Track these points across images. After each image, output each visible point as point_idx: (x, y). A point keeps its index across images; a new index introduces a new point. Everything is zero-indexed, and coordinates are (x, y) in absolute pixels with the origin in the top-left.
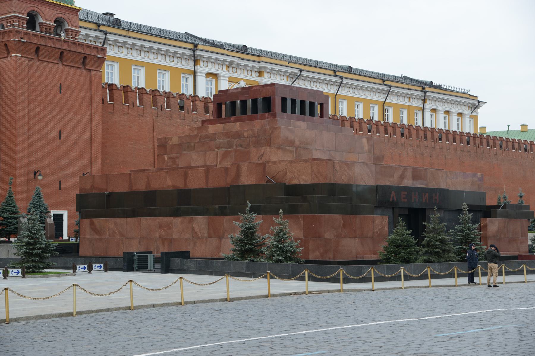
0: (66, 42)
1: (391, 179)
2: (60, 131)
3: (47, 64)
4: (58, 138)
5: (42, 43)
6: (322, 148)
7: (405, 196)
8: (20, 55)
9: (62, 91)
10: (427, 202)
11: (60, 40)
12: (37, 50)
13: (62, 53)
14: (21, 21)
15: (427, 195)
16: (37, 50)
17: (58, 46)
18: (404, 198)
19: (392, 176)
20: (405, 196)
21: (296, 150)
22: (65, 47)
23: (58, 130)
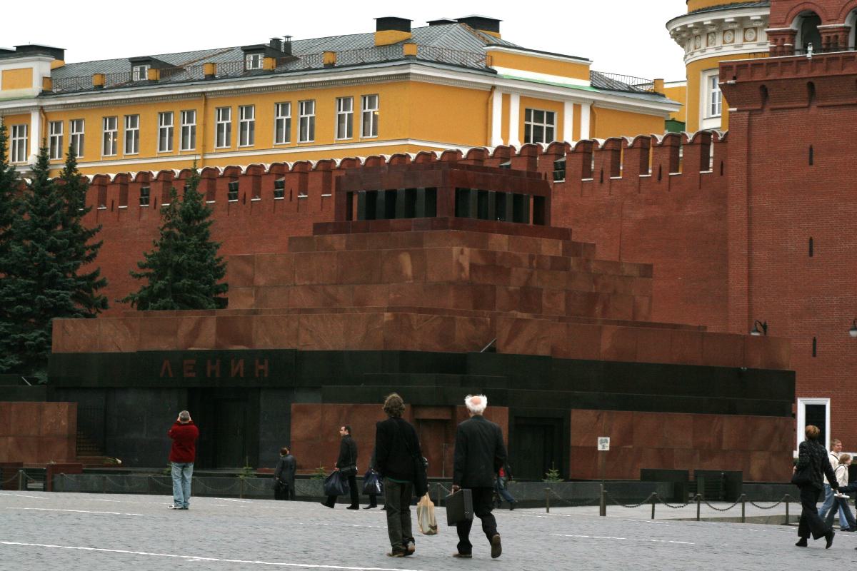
0: (815, 60)
1: (172, 340)
2: (811, 240)
3: (785, 113)
4: (807, 253)
5: (771, 77)
6: (307, 283)
7: (191, 368)
8: (735, 109)
9: (815, 160)
10: (242, 375)
11: (805, 60)
12: (764, 90)
14: (780, 39)
15: (241, 363)
16: (764, 90)
17: (804, 74)
18: (189, 371)
19: (174, 333)
20: (191, 368)
21: (257, 292)
22: (817, 73)
23: (807, 238)
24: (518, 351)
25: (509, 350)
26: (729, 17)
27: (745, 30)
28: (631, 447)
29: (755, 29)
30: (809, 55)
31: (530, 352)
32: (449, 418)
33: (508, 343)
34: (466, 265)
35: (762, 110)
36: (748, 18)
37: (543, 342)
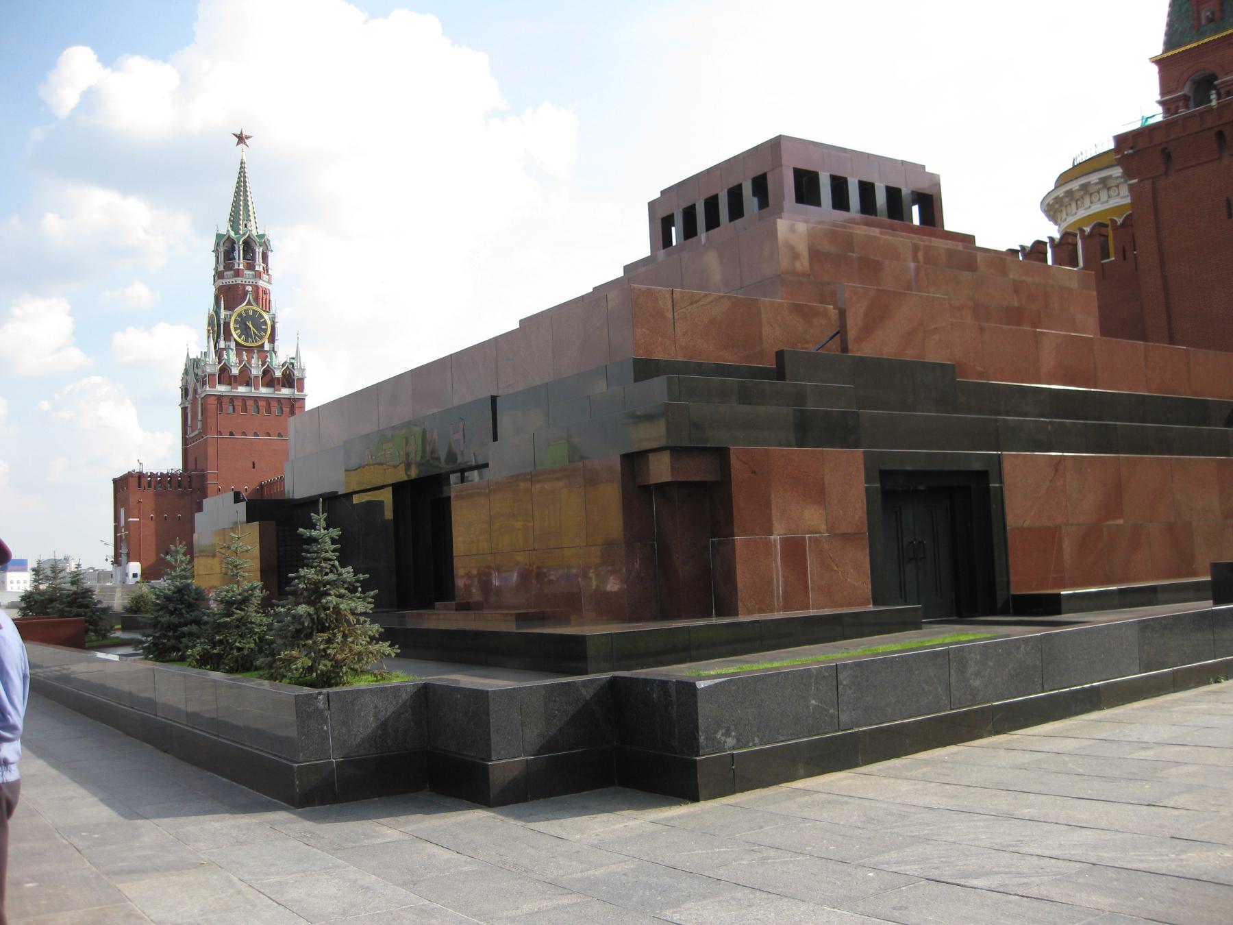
0: (1221, 107)
5: (1172, 137)
11: (1211, 109)
13: (1220, 135)
14: (1173, 107)
24: (887, 352)
25: (866, 350)
26: (1094, 178)
27: (1109, 189)
28: (1121, 521)
29: (1117, 186)
30: (1214, 103)
31: (910, 355)
32: (710, 478)
33: (868, 329)
34: (803, 248)
35: (1166, 174)
36: (1110, 176)
37: (936, 337)
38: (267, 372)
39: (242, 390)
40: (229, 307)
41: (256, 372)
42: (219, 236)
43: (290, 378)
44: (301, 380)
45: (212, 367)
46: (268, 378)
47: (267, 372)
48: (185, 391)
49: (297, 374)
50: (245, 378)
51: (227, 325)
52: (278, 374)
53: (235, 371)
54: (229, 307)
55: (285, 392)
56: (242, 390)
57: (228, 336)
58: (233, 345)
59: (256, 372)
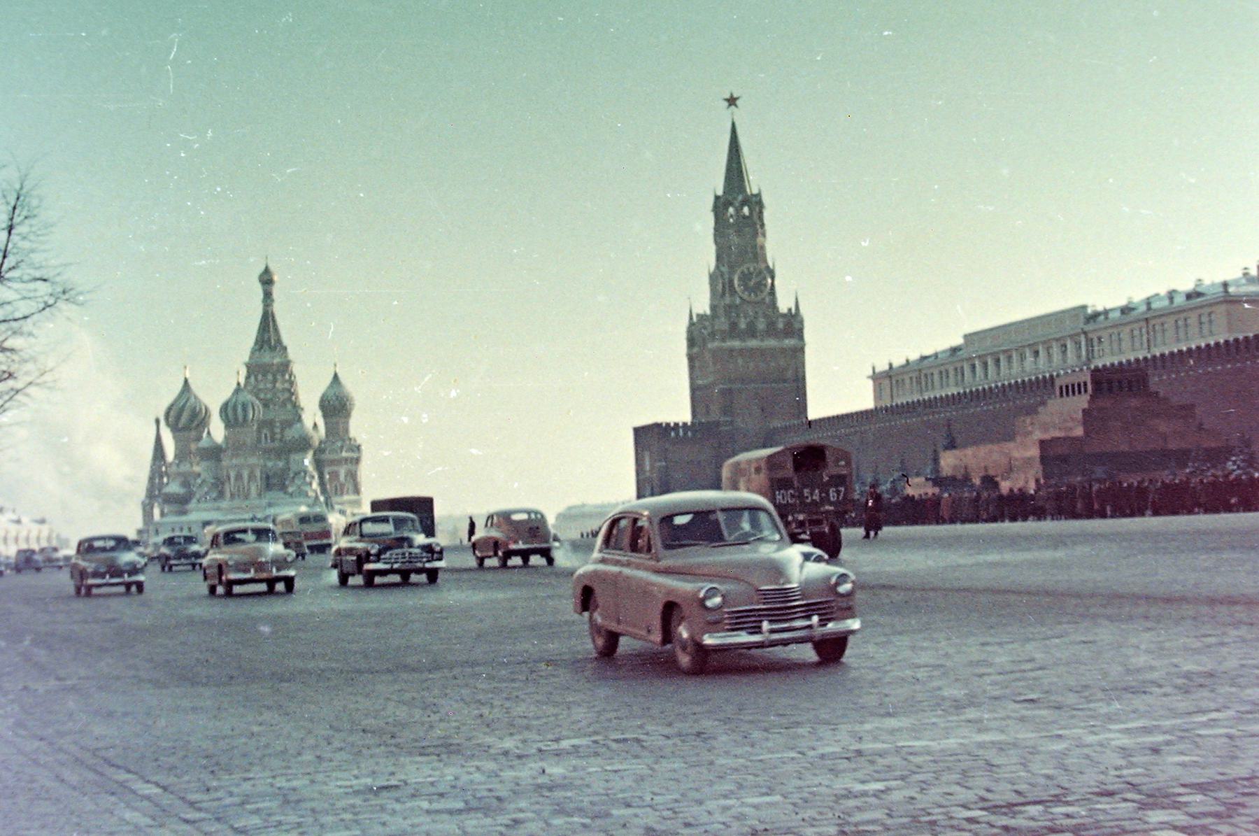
38: (771, 325)
39: (753, 343)
40: (732, 268)
41: (761, 325)
42: (717, 198)
43: (792, 325)
44: (801, 330)
45: (722, 324)
46: (771, 331)
47: (771, 325)
48: (691, 342)
49: (797, 326)
50: (752, 332)
51: (731, 281)
52: (781, 326)
53: (743, 326)
54: (732, 268)
55: (789, 342)
56: (753, 343)
57: (733, 291)
58: (738, 301)
59: (761, 325)
